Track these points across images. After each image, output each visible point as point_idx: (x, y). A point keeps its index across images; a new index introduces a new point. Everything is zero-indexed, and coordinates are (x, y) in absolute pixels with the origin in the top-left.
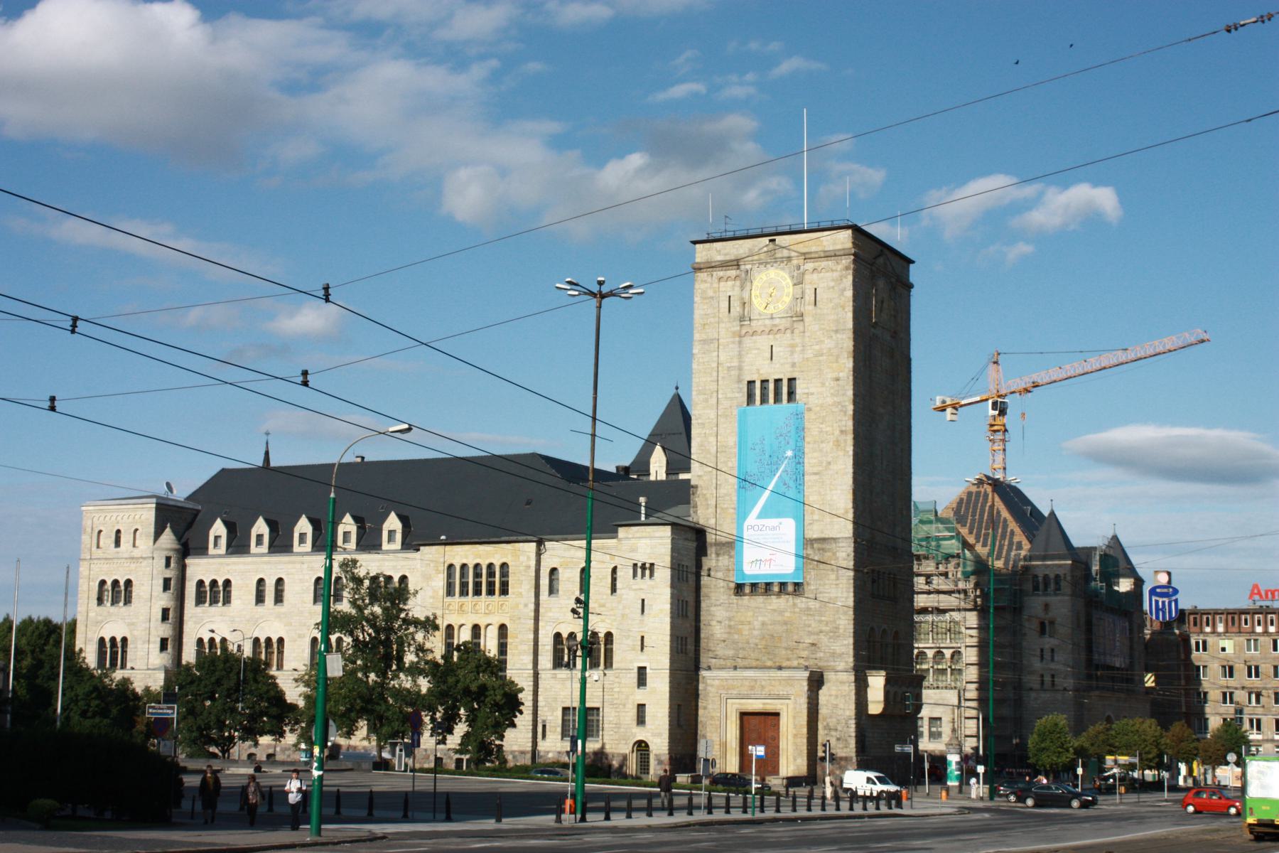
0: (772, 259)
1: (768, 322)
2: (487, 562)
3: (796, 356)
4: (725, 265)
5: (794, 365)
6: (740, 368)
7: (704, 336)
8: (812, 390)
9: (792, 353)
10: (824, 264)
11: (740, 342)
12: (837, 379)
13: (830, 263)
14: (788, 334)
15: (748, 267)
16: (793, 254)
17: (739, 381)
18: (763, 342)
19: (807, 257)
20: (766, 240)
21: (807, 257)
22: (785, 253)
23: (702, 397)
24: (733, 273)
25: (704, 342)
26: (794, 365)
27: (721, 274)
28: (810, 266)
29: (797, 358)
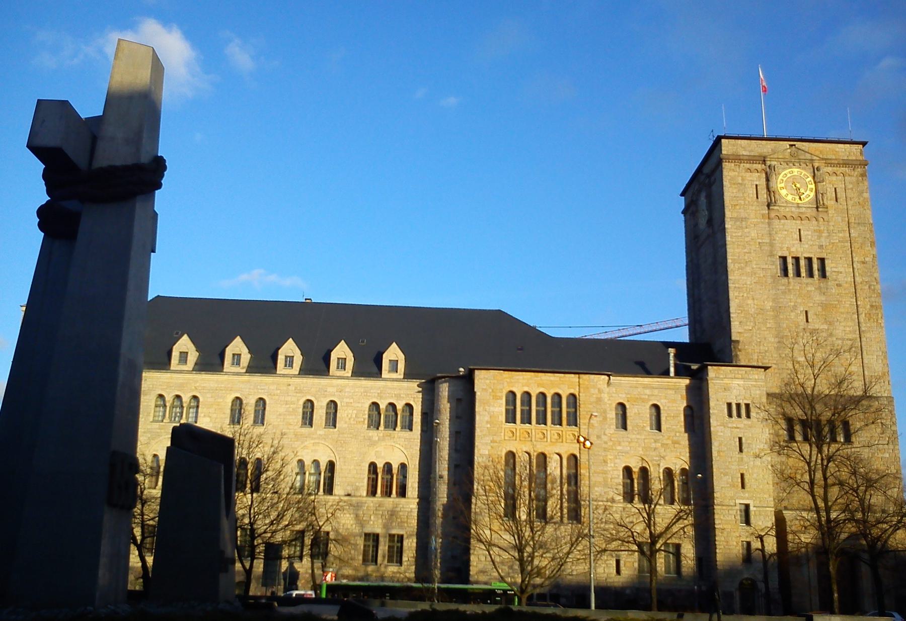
0: (794, 160)
1: (793, 209)
2: (553, 391)
3: (823, 239)
4: (752, 160)
5: (821, 247)
6: (771, 245)
7: (735, 215)
8: (842, 270)
9: (819, 237)
10: (840, 170)
11: (769, 224)
12: (863, 263)
13: (846, 170)
14: (815, 222)
15: (773, 163)
16: (815, 158)
17: (771, 255)
18: (792, 226)
19: (828, 162)
20: (786, 144)
21: (828, 162)
22: (808, 156)
23: (737, 266)
24: (759, 167)
25: (736, 219)
26: (821, 247)
27: (748, 166)
28: (829, 169)
29: (824, 241)
